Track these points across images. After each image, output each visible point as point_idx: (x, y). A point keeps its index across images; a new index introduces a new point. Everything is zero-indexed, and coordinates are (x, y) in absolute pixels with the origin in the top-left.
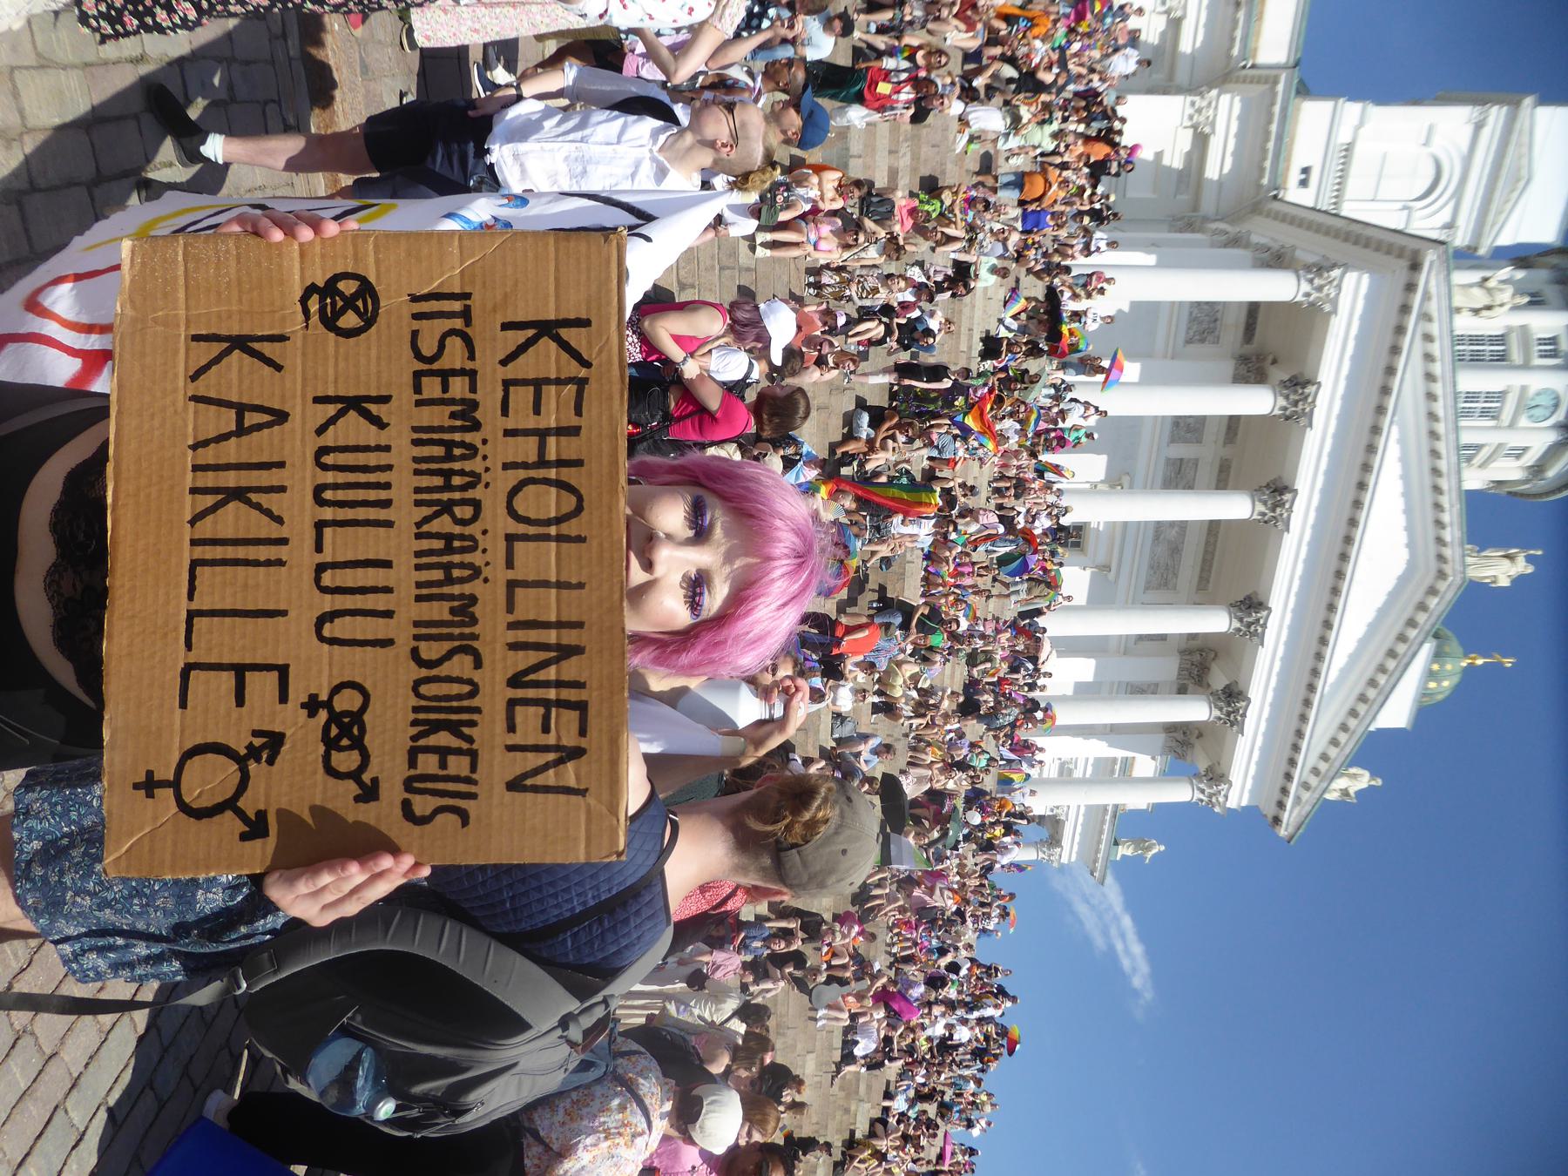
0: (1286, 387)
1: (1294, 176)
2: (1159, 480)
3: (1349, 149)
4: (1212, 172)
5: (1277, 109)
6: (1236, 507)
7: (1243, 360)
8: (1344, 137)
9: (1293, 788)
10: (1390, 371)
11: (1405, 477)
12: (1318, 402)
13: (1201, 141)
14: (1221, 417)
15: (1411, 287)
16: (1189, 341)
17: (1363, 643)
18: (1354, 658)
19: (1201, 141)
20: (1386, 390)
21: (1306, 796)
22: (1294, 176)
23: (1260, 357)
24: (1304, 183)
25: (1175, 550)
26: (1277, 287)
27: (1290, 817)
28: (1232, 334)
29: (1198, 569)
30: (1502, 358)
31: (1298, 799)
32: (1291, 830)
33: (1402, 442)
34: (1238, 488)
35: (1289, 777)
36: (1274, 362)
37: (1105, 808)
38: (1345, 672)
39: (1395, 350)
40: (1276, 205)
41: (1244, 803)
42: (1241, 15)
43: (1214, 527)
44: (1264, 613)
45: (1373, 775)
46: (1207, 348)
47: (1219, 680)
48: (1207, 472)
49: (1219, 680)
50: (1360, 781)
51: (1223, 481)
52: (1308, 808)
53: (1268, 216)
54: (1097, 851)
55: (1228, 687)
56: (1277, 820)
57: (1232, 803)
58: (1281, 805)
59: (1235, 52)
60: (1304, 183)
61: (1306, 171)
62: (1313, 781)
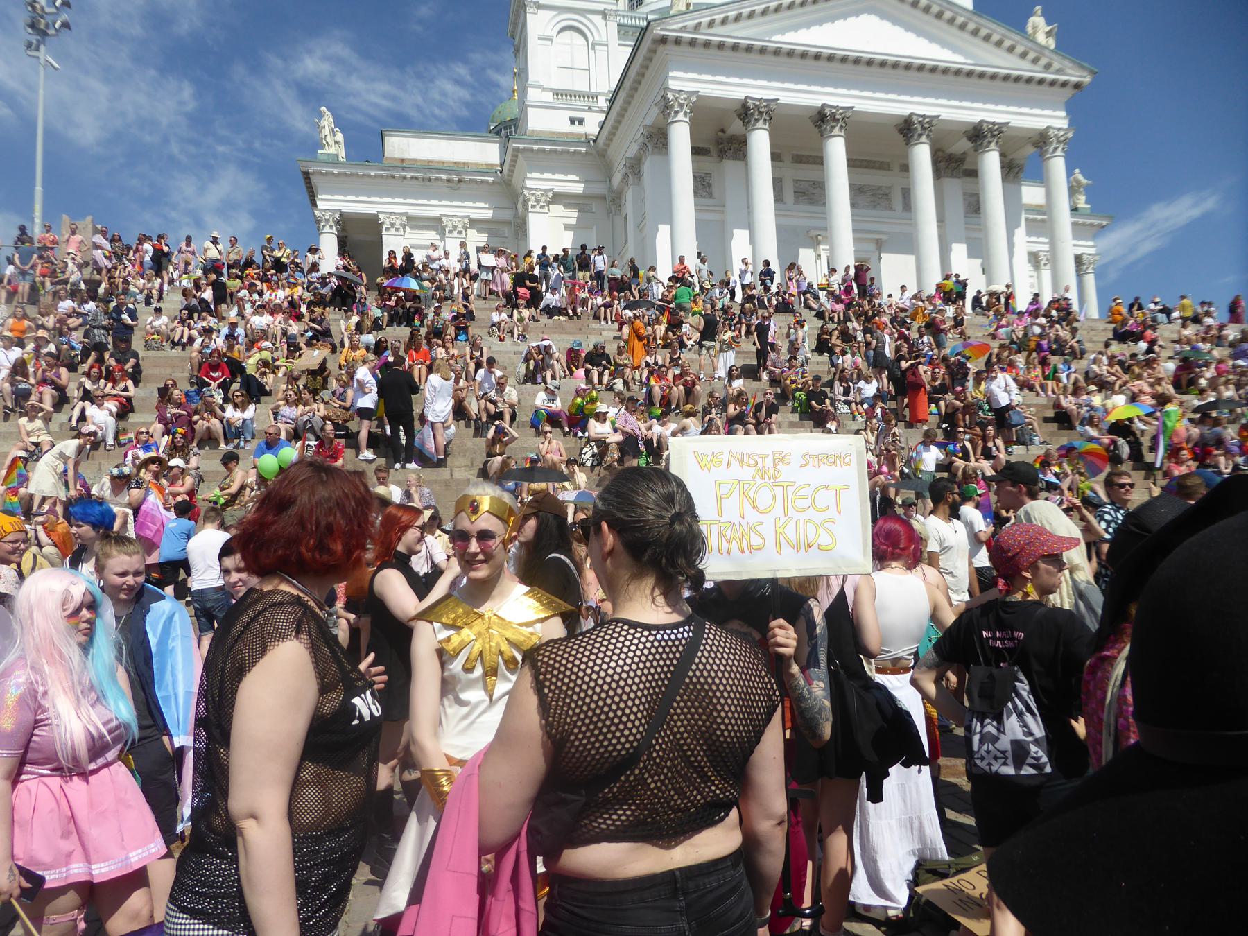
0: (749, 122)
1: (577, 129)
3: (557, 93)
4: (579, 188)
5: (535, 147)
6: (837, 149)
7: (722, 154)
8: (548, 97)
9: (1051, 77)
10: (735, 47)
11: (808, 25)
12: (759, 97)
13: (557, 198)
14: (849, 173)
15: (678, 41)
16: (711, 195)
17: (932, 39)
18: (944, 44)
19: (557, 198)
20: (749, 49)
21: (1056, 66)
22: (577, 129)
23: (719, 142)
24: (581, 121)
26: (681, 136)
27: (1074, 75)
28: (708, 163)
29: (874, 171)
31: (1059, 71)
32: (1085, 74)
33: (783, 31)
34: (821, 149)
35: (1041, 82)
36: (723, 131)
37: (1074, 224)
38: (955, 50)
39: (721, 46)
40: (601, 141)
41: (1063, 114)
42: (468, 178)
43: (852, 163)
44: (914, 118)
45: (1032, 14)
47: (964, 145)
48: (807, 173)
49: (964, 145)
50: (1038, 24)
51: (818, 160)
52: (1067, 63)
53: (608, 145)
54: (1084, 224)
55: (970, 139)
56: (1077, 86)
57: (1064, 124)
58: (1064, 84)
59: (491, 179)
60: (581, 121)
61: (572, 121)
62: (1044, 61)
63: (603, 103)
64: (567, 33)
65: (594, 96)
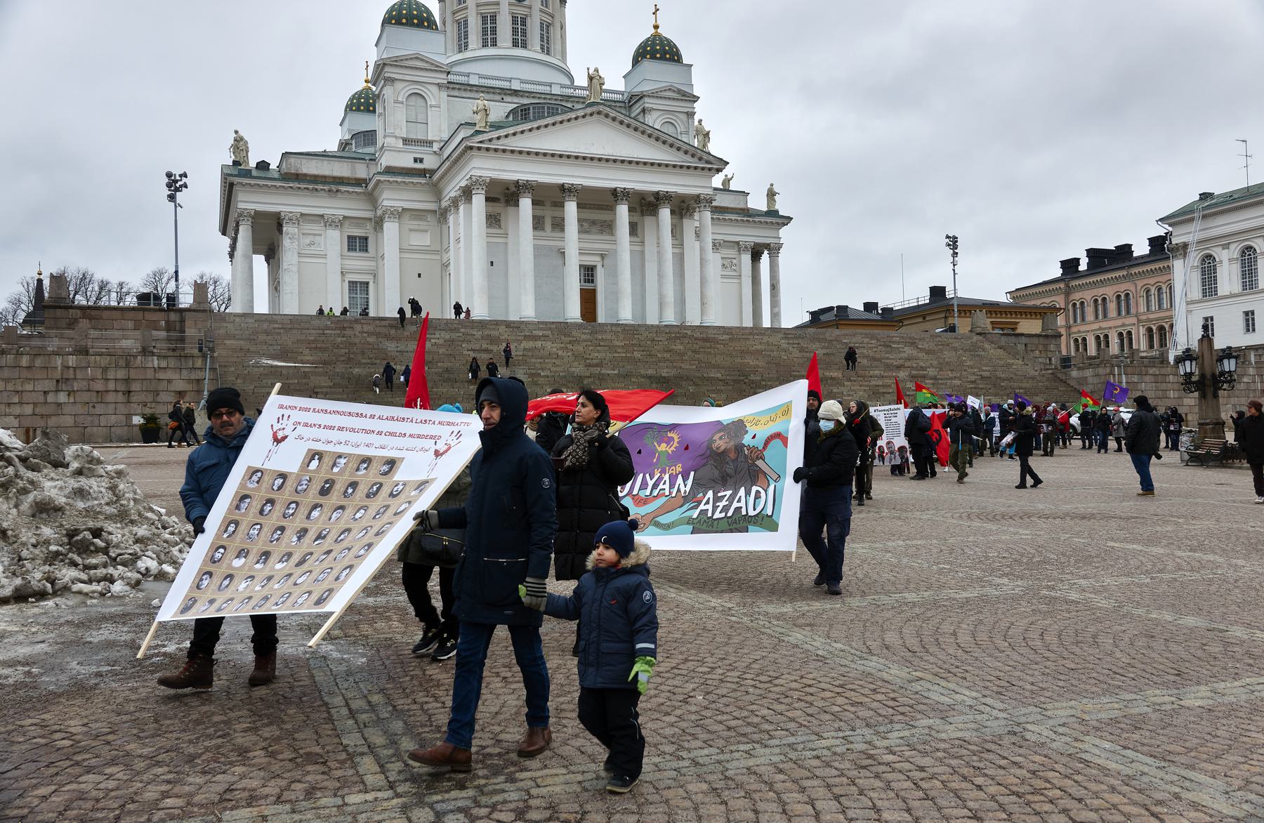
2: (559, 235)
3: (406, 141)
6: (571, 208)
8: (400, 144)
15: (479, 149)
16: (500, 227)
22: (418, 166)
23: (506, 195)
24: (421, 161)
25: (593, 223)
26: (479, 200)
28: (498, 208)
30: (494, 18)
31: (708, 162)
35: (696, 168)
40: (436, 177)
46: (502, 219)
61: (415, 160)
63: (436, 147)
64: (413, 98)
65: (430, 143)
